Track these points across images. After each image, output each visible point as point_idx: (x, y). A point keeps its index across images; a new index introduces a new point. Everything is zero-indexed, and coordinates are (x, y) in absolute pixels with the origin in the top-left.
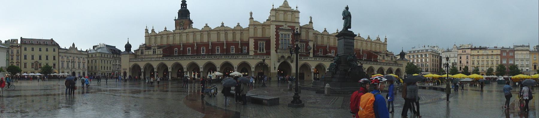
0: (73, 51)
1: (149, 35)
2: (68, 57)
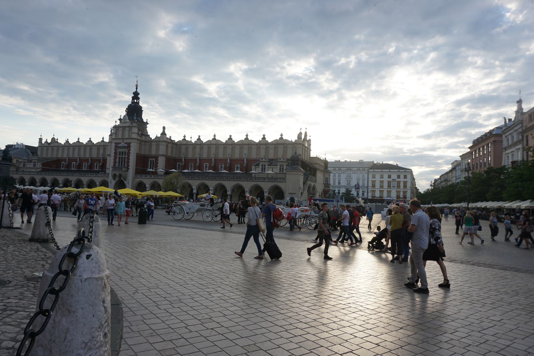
1: (42, 145)
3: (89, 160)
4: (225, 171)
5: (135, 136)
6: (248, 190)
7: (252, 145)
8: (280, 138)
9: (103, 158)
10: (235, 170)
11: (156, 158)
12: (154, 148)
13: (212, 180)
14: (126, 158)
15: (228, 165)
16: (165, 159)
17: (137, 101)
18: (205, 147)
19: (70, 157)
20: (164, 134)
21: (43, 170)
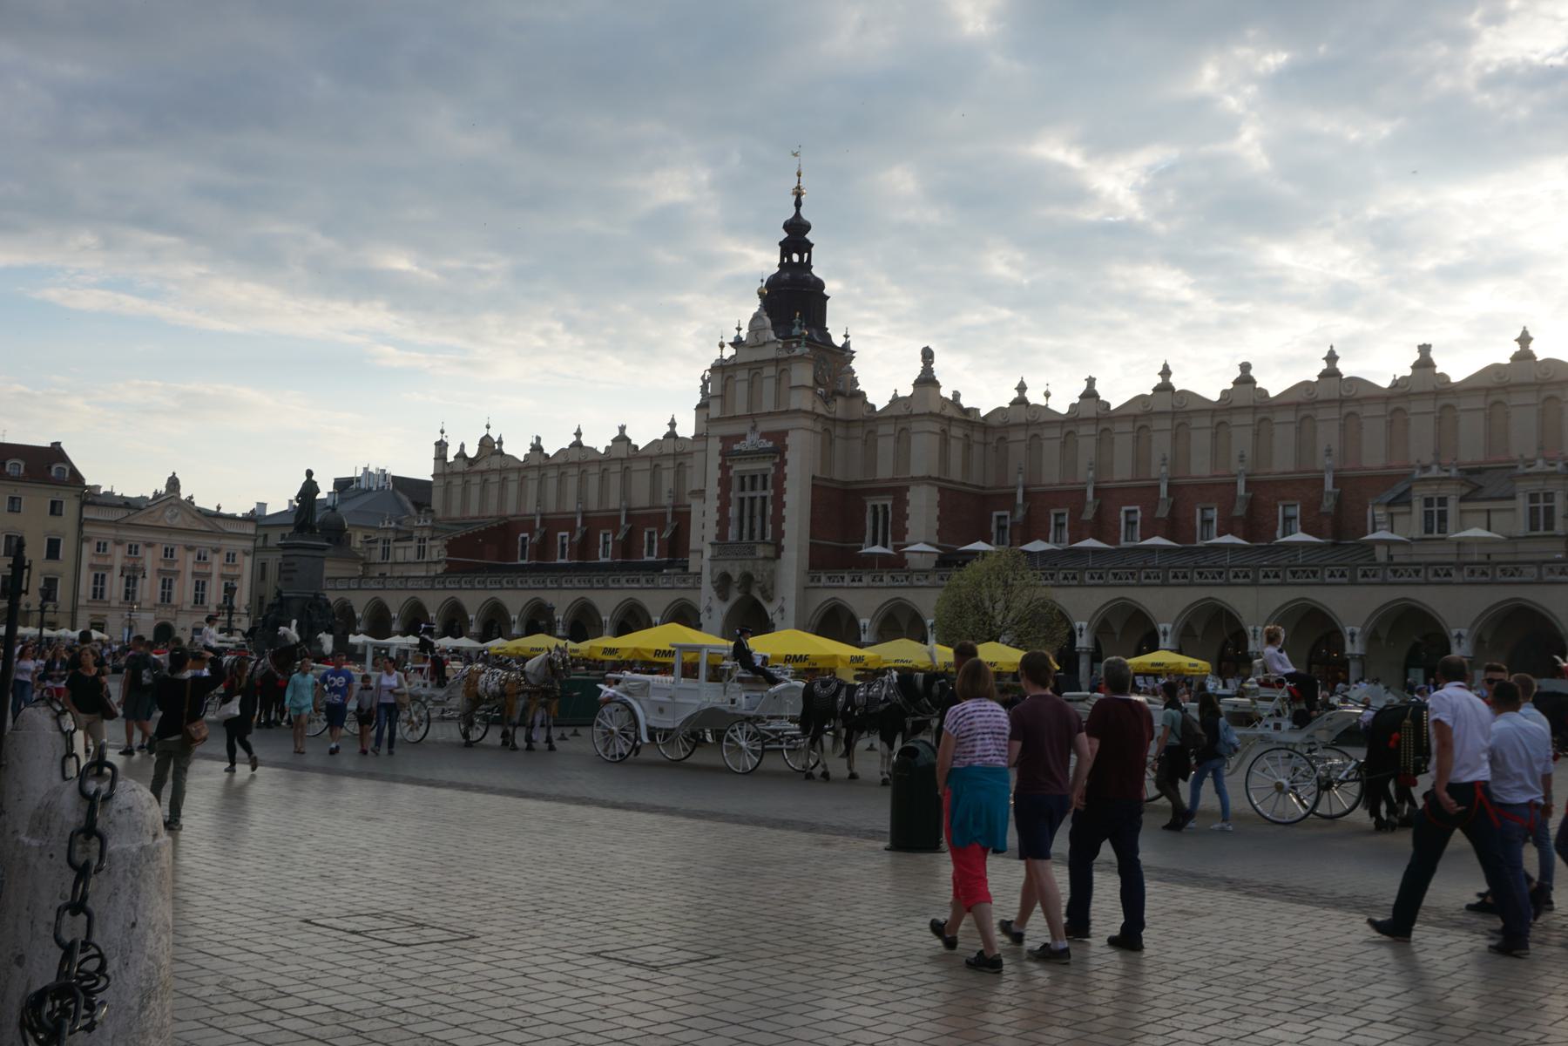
0: (167, 518)
1: (448, 470)
2: (133, 549)
3: (619, 517)
4: (1228, 539)
5: (802, 401)
6: (1358, 630)
7: (1359, 401)
8: (1516, 358)
9: (674, 507)
10: (1279, 533)
11: (898, 492)
12: (886, 446)
13: (1164, 584)
14: (769, 501)
15: (1239, 510)
16: (937, 497)
17: (801, 258)
18: (1118, 427)
19: (548, 511)
20: (927, 380)
21: (453, 569)
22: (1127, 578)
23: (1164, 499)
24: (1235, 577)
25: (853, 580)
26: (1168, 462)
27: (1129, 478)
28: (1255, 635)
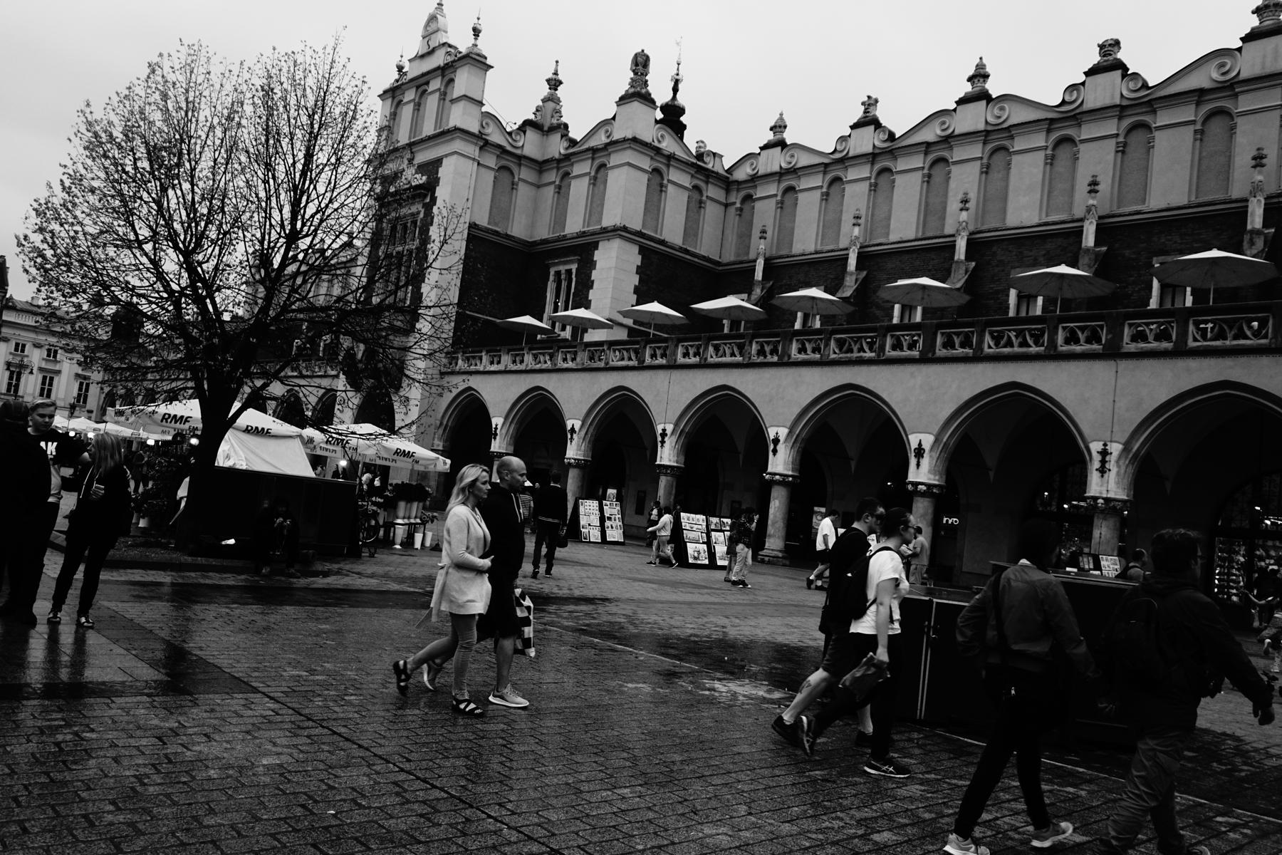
13: (927, 358)
16: (637, 260)
22: (861, 350)
23: (959, 262)
24: (1067, 342)
25: (492, 363)
26: (971, 205)
27: (912, 236)
28: (1103, 462)
